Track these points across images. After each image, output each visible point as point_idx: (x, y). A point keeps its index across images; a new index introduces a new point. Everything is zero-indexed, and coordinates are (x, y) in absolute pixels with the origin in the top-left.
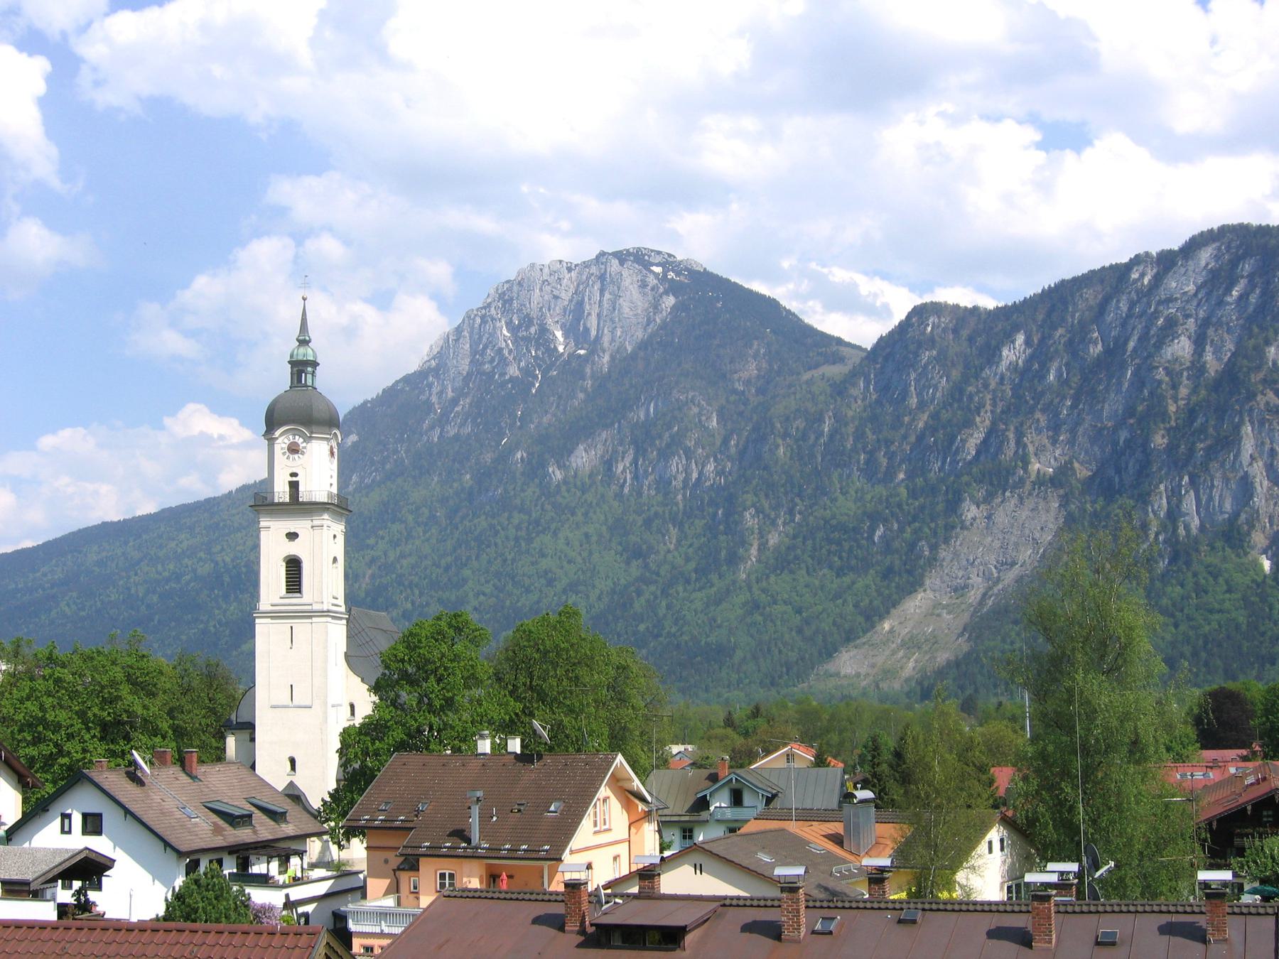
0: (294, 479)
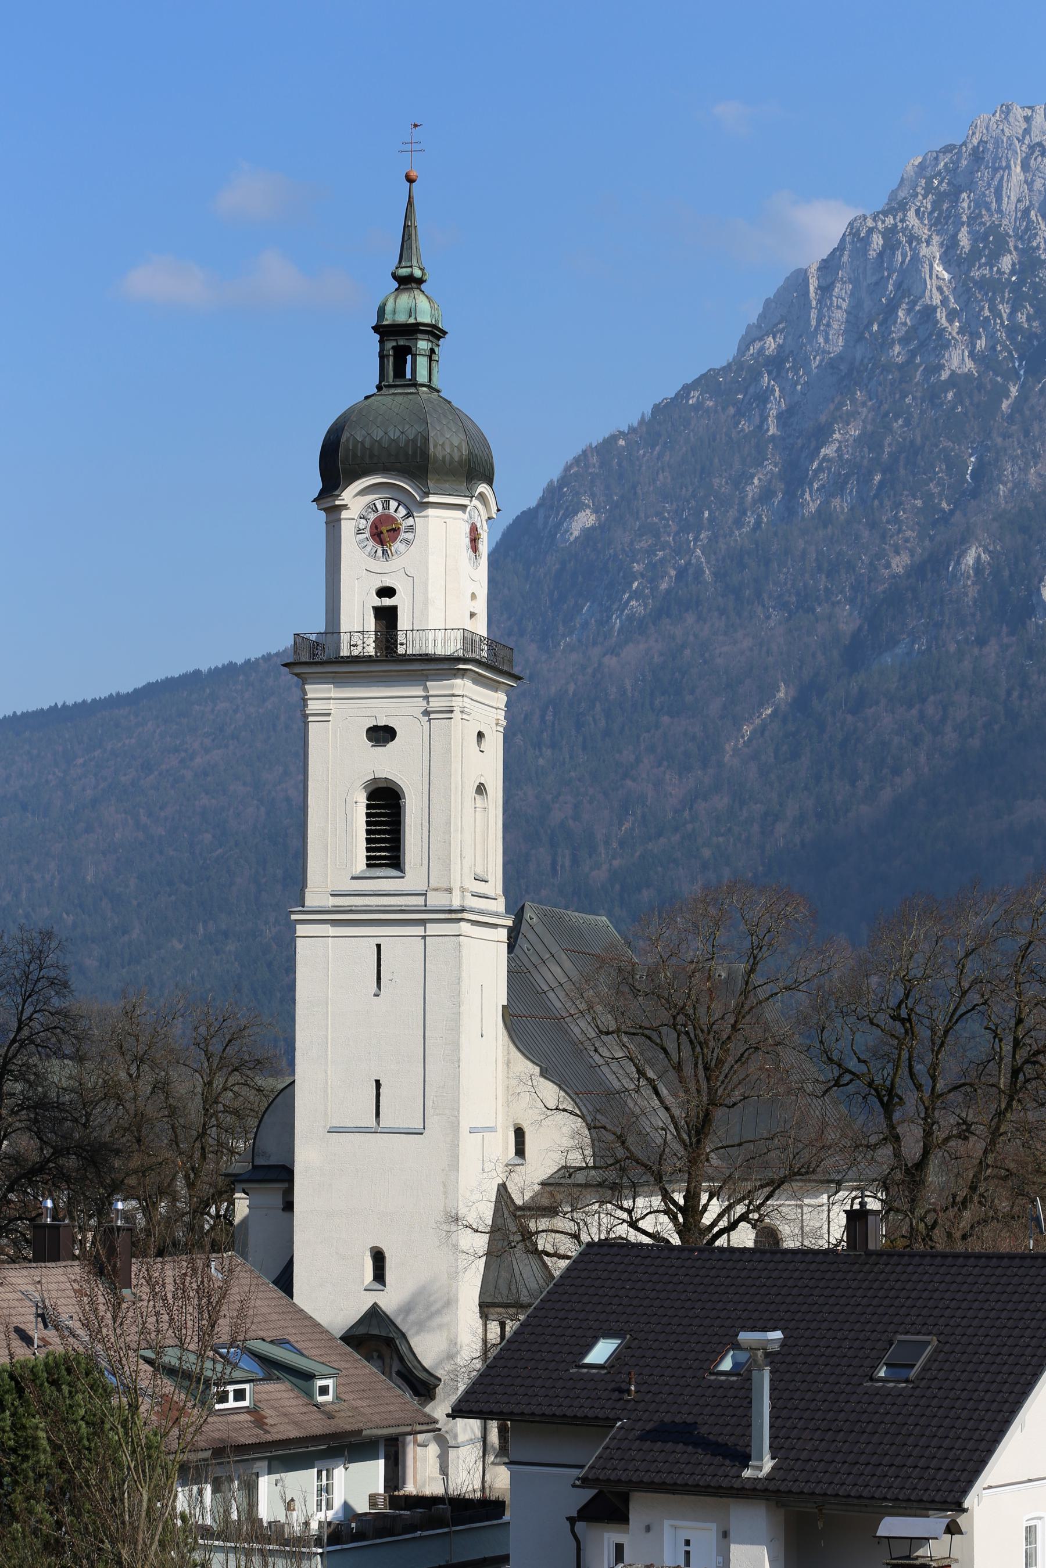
0: (387, 602)
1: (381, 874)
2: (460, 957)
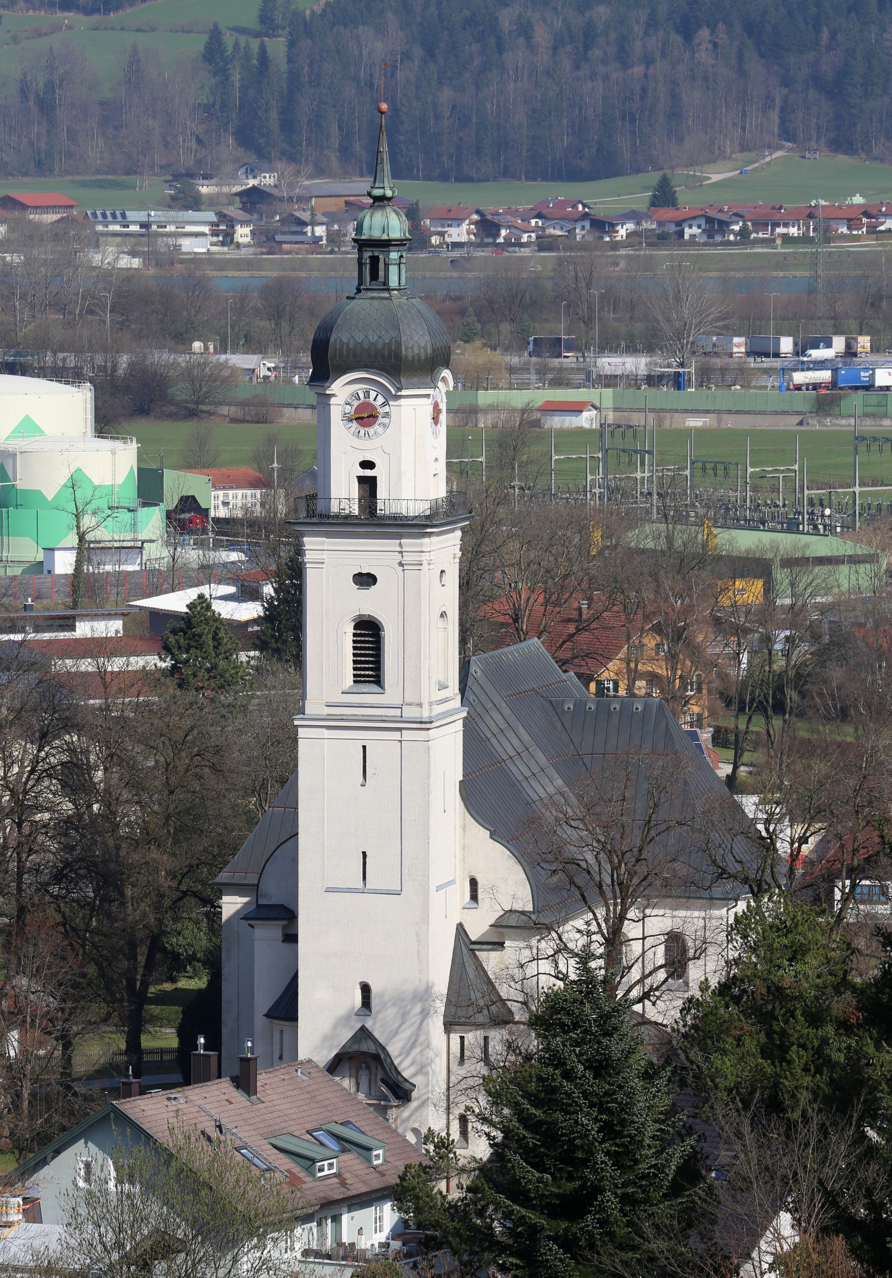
0: (368, 473)
1: (366, 690)
2: (429, 758)
